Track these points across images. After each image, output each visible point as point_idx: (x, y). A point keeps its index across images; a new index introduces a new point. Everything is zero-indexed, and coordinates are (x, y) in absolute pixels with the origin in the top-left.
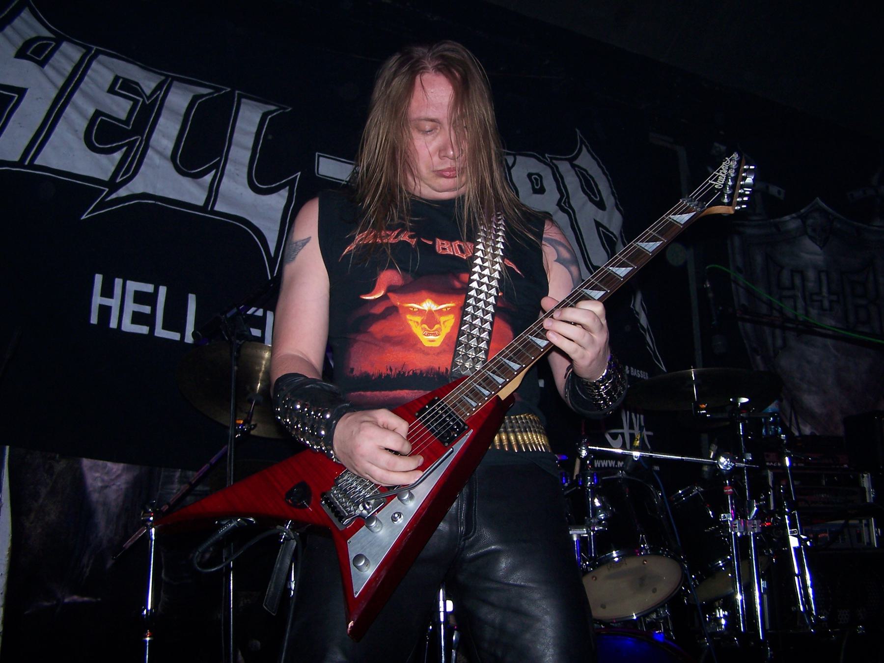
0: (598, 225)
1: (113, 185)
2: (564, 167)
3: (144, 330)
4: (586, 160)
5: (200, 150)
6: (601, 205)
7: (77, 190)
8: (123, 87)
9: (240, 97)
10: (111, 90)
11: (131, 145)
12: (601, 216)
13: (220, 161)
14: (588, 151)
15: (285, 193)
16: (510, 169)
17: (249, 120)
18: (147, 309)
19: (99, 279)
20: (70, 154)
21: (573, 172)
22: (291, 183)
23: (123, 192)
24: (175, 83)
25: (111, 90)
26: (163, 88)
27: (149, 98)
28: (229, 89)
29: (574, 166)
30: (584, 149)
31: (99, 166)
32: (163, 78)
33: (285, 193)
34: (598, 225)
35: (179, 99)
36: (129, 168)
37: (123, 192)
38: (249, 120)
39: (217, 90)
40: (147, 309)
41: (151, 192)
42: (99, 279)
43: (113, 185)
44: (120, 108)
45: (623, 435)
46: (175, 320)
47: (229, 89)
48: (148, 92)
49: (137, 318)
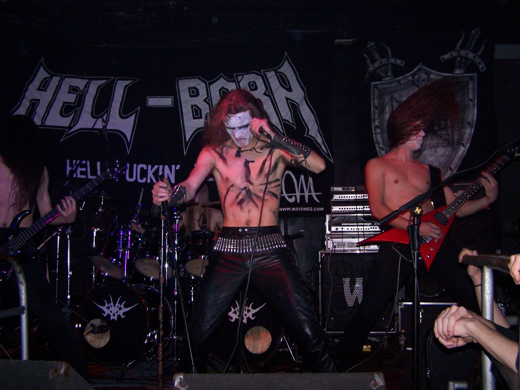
0: (287, 99)
1: (70, 128)
2: (271, 76)
3: (84, 177)
4: (286, 69)
5: (101, 107)
6: (290, 90)
7: (59, 131)
8: (73, 89)
9: (118, 80)
10: (69, 92)
11: (76, 112)
12: (290, 95)
13: (108, 110)
14: (289, 62)
15: (133, 117)
16: (239, 82)
17: (120, 89)
18: (84, 169)
19: (68, 161)
20: (56, 120)
21: (275, 76)
22: (136, 112)
23: (72, 130)
24: (93, 82)
25: (69, 92)
26: (87, 86)
27: (81, 92)
28: (113, 78)
29: (276, 73)
30: (286, 63)
31: (65, 122)
32: (88, 80)
33: (133, 117)
34: (287, 99)
35: (93, 90)
36: (75, 121)
37: (72, 130)
38: (120, 89)
39: (108, 79)
40: (84, 169)
41: (83, 127)
42: (68, 161)
43: (70, 128)
44: (72, 98)
45: (295, 196)
46: (94, 172)
47: (113, 78)
48: (81, 89)
49: (82, 173)
